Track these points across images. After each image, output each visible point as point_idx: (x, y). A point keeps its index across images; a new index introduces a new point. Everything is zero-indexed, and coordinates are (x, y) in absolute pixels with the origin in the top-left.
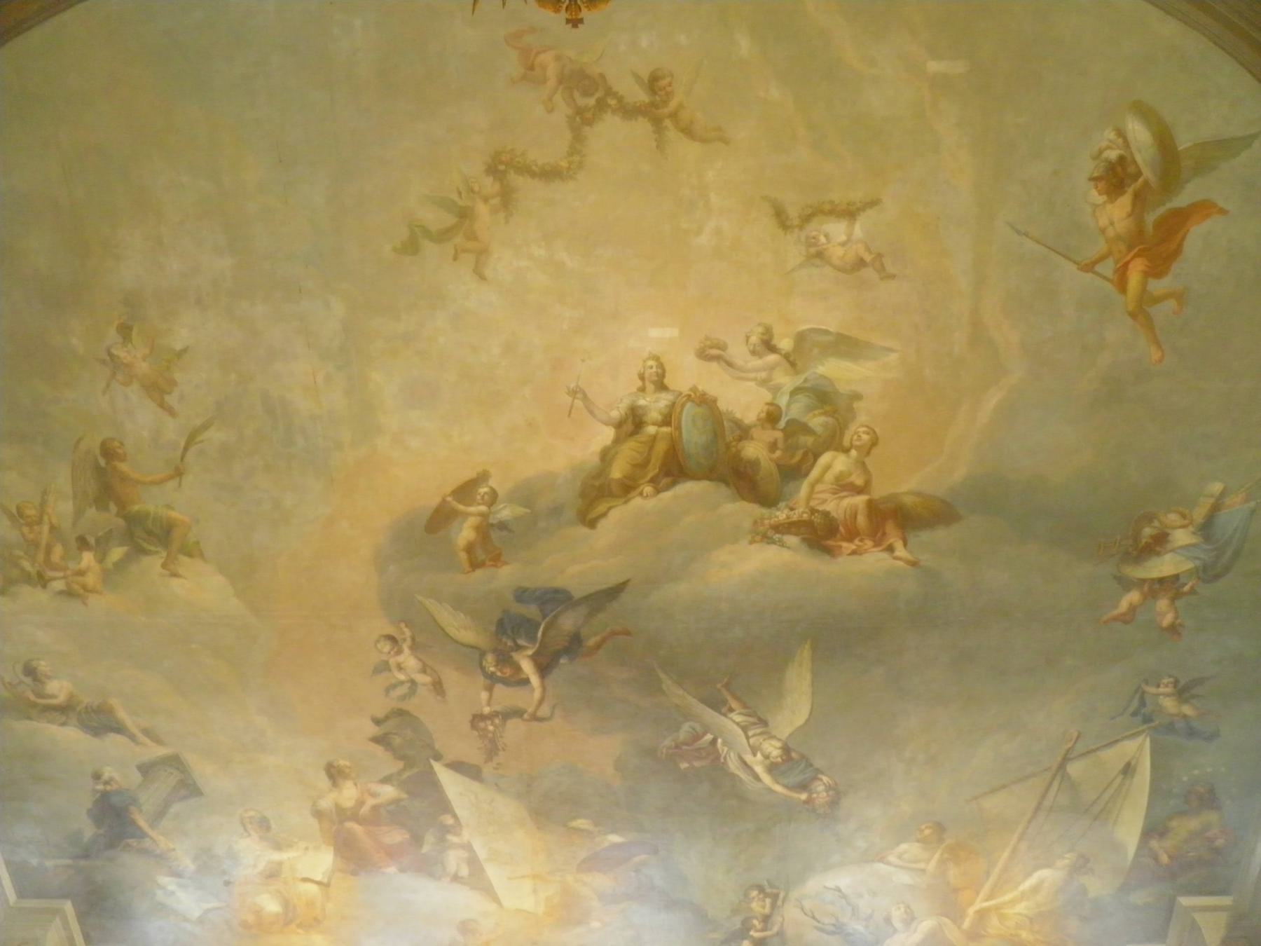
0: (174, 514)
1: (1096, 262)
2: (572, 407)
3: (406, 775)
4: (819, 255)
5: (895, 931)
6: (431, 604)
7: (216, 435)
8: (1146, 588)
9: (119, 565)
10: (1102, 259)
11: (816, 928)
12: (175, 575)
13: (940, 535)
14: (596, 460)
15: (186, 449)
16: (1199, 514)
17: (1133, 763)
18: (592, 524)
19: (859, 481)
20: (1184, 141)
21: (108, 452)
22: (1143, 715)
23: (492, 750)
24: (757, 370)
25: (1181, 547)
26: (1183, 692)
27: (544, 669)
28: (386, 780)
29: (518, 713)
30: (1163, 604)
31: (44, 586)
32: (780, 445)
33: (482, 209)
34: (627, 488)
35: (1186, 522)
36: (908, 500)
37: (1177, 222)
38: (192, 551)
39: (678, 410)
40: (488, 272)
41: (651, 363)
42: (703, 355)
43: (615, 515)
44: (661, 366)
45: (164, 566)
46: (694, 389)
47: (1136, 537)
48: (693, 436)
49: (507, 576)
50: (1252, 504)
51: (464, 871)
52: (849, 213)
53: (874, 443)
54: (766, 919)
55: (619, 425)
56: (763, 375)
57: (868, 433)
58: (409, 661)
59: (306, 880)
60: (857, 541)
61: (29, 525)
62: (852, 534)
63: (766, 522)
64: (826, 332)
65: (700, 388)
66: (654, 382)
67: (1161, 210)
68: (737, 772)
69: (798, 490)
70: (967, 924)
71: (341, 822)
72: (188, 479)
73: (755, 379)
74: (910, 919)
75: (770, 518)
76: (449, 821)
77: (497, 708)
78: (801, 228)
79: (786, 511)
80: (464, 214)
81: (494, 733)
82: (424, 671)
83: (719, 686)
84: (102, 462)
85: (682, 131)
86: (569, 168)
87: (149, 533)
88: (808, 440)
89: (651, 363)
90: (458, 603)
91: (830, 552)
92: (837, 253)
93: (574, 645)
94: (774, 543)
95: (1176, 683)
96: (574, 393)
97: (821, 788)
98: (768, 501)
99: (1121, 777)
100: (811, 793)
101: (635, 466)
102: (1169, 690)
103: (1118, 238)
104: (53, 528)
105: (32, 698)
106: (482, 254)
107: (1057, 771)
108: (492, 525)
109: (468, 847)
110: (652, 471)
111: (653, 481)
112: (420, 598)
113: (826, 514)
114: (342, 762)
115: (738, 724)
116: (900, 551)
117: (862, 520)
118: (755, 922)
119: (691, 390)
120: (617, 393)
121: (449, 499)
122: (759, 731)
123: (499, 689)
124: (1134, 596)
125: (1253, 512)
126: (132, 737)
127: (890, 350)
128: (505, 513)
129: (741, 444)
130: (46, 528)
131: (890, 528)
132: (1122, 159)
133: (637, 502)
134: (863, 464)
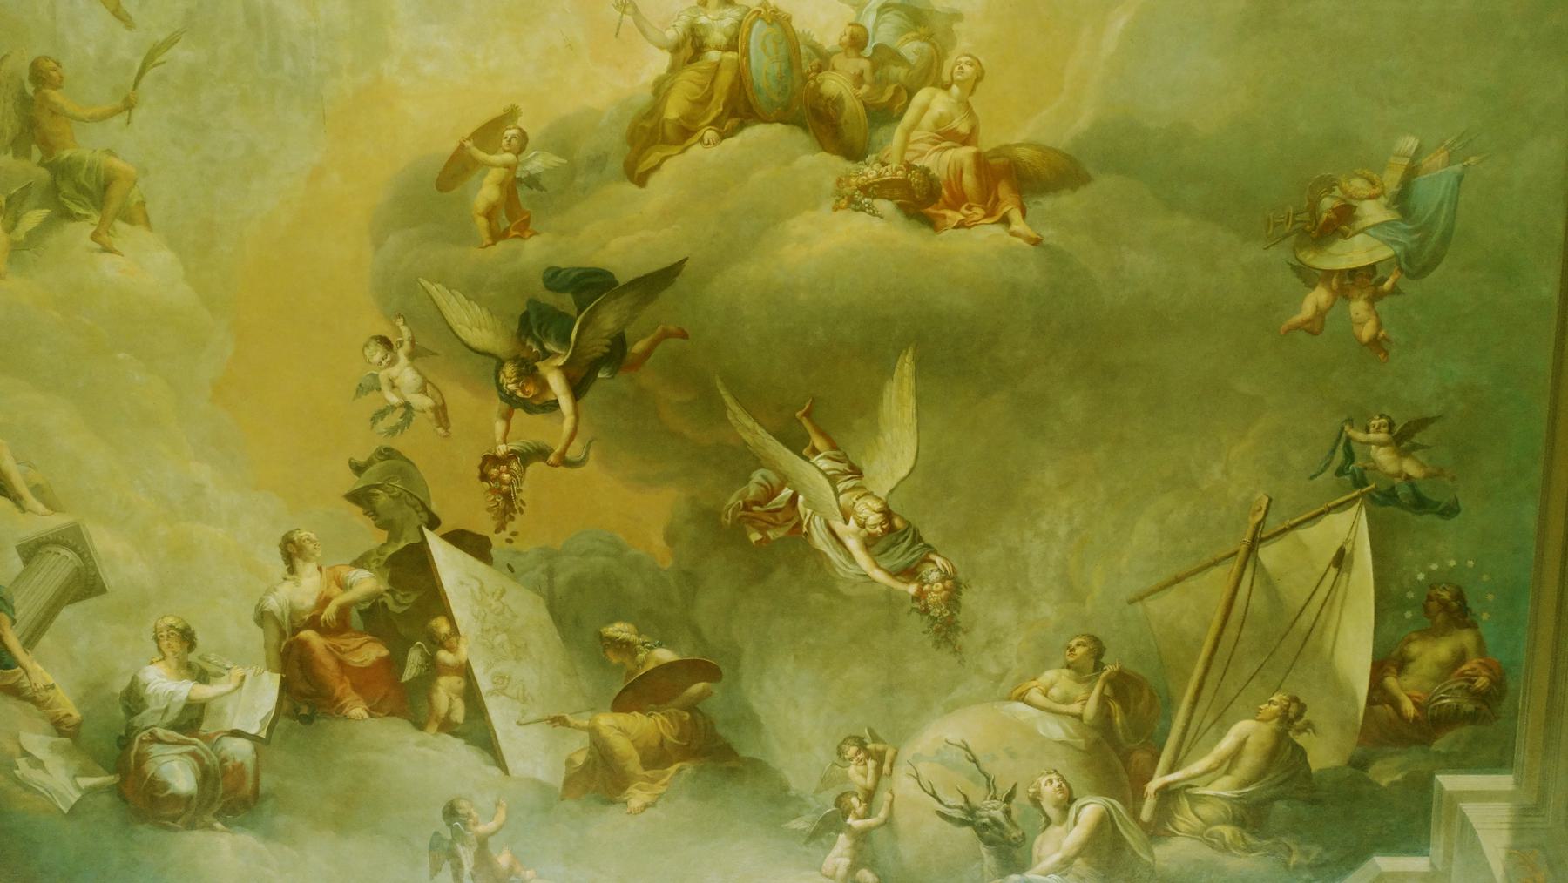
0: (117, 163)
3: (391, 551)
5: (1048, 822)
6: (436, 290)
7: (182, 54)
9: (34, 237)
12: (107, 249)
13: (1066, 202)
15: (141, 73)
16: (1392, 180)
17: (1348, 548)
18: (641, 181)
19: (964, 128)
21: (39, 75)
22: (1354, 478)
23: (507, 506)
25: (1374, 226)
26: (1402, 440)
28: (359, 563)
29: (541, 453)
30: (1358, 307)
32: (867, 76)
34: (686, 132)
35: (1377, 191)
36: (1024, 154)
39: (746, 30)
43: (670, 169)
45: (94, 237)
47: (1313, 209)
48: (764, 66)
49: (535, 251)
50: (1458, 168)
51: (459, 714)
53: (979, 78)
54: (869, 796)
55: (676, 49)
58: (405, 374)
59: (237, 734)
60: (963, 209)
63: (853, 181)
68: (824, 548)
69: (890, 139)
70: (1146, 814)
71: (296, 631)
72: (139, 113)
74: (1068, 802)
76: (442, 626)
79: (876, 166)
81: (511, 483)
83: (799, 414)
84: (30, 89)
87: (81, 189)
88: (899, 72)
90: (473, 290)
91: (931, 223)
93: (617, 353)
95: (1391, 425)
97: (934, 576)
98: (854, 153)
99: (1333, 571)
101: (694, 103)
102: (1382, 436)
108: (520, 180)
109: (465, 671)
110: (715, 110)
112: (425, 283)
113: (925, 171)
114: (304, 534)
115: (823, 472)
116: (1018, 225)
117: (969, 180)
118: (854, 800)
121: (468, 144)
122: (851, 483)
123: (519, 415)
124: (1319, 297)
125: (1460, 178)
126: (17, 500)
128: (537, 163)
131: (1003, 190)
133: (696, 150)
134: (968, 106)
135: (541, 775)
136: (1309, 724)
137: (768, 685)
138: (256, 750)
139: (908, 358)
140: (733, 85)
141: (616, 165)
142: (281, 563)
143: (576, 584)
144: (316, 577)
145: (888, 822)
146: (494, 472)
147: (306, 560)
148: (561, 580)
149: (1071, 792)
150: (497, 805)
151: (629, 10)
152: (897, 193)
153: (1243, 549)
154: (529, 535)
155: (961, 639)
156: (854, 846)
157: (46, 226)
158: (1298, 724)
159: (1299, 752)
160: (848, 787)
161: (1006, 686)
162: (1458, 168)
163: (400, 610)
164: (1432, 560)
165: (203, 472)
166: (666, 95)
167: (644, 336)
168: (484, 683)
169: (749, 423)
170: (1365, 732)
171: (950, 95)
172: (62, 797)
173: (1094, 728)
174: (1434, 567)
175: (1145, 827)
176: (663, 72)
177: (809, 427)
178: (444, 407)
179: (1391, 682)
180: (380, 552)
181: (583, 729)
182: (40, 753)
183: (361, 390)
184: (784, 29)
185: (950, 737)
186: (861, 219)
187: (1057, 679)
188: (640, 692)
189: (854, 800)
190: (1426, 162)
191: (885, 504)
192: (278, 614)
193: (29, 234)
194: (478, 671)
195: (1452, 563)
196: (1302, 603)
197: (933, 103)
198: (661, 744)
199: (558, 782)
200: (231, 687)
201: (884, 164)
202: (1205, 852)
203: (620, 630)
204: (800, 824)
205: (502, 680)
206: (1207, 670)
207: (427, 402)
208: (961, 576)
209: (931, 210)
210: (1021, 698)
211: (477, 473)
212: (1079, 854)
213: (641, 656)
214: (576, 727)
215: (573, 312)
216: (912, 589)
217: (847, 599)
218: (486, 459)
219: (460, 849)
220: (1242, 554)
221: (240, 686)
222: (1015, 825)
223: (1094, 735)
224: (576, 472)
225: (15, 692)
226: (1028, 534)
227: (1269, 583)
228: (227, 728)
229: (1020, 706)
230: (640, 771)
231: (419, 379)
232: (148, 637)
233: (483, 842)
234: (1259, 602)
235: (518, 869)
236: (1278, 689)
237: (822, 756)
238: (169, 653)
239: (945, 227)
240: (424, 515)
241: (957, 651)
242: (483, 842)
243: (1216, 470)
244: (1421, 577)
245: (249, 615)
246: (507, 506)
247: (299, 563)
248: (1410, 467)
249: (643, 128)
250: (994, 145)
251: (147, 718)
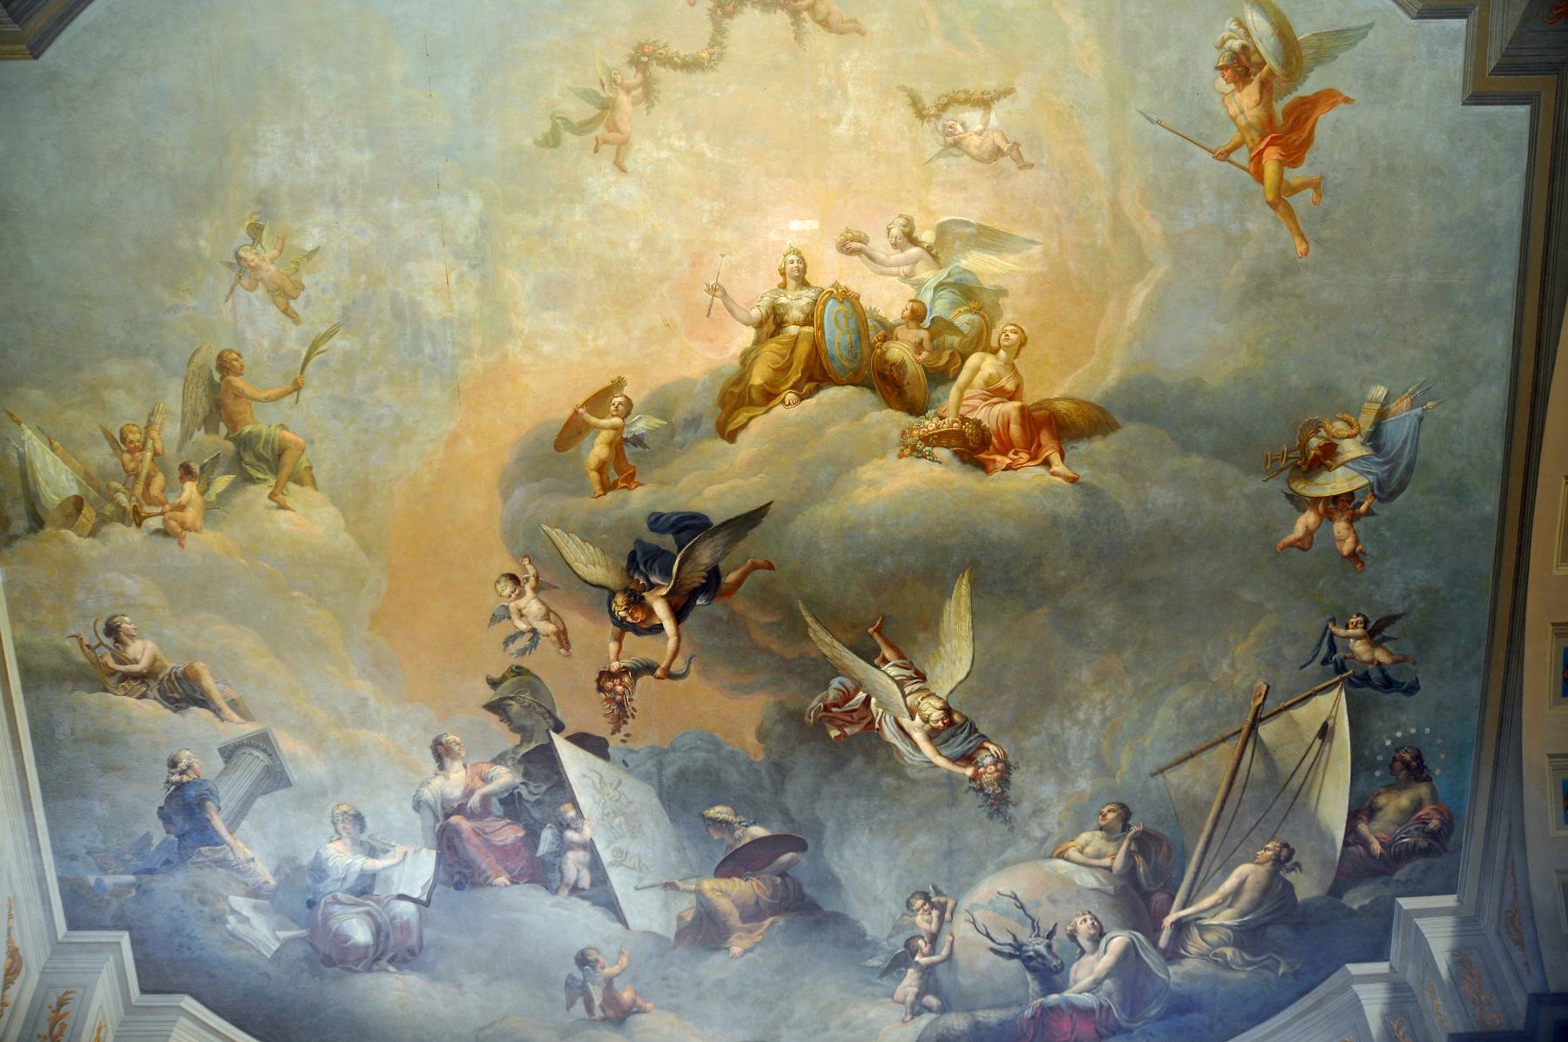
0: (287, 435)
1: (1229, 152)
3: (524, 750)
4: (957, 144)
5: (1083, 952)
6: (557, 535)
7: (340, 343)
8: (1321, 507)
9: (223, 497)
10: (1236, 147)
11: (992, 949)
12: (282, 507)
13: (1098, 446)
14: (736, 364)
15: (307, 360)
16: (1366, 422)
17: (1330, 723)
18: (731, 437)
19: (1010, 386)
20: (1303, 32)
21: (224, 365)
23: (621, 713)
25: (1352, 460)
26: (1374, 634)
27: (679, 614)
28: (495, 762)
31: (139, 525)
32: (926, 344)
33: (624, 100)
34: (769, 395)
36: (1062, 406)
37: (1303, 113)
38: (302, 478)
40: (628, 164)
41: (791, 257)
43: (755, 426)
44: (802, 260)
45: (271, 496)
46: (836, 285)
47: (1303, 447)
48: (837, 338)
49: (640, 500)
50: (1418, 411)
51: (585, 881)
52: (984, 102)
53: (1023, 343)
54: (934, 939)
55: (759, 325)
56: (906, 269)
58: (531, 604)
59: (402, 897)
60: (1011, 454)
61: (130, 451)
62: (1006, 447)
64: (968, 224)
66: (795, 279)
67: (1288, 99)
68: (893, 741)
70: (1163, 942)
71: (447, 816)
72: (306, 394)
74: (1099, 935)
77: (626, 662)
78: (938, 117)
80: (607, 106)
82: (547, 617)
84: (217, 377)
85: (819, 22)
86: (710, 60)
87: (259, 457)
88: (953, 340)
89: (791, 257)
90: (588, 533)
91: (983, 466)
92: (973, 142)
95: (1366, 622)
96: (712, 290)
97: (988, 760)
98: (916, 409)
99: (1318, 742)
100: (977, 766)
102: (1359, 631)
103: (1250, 126)
104: (156, 454)
105: (111, 663)
106: (623, 145)
107: (1249, 735)
108: (626, 440)
109: (589, 847)
110: (795, 376)
112: (546, 528)
113: (978, 423)
114: (451, 738)
115: (892, 678)
116: (1058, 466)
117: (1015, 429)
118: (921, 942)
120: (757, 289)
121: (581, 410)
122: (917, 686)
123: (629, 637)
124: (1309, 519)
125: (1421, 419)
126: (217, 712)
128: (640, 425)
130: (149, 455)
131: (1045, 437)
132: (1244, 48)
133: (779, 410)
135: (656, 928)
136: (1297, 864)
137: (847, 853)
138: (420, 911)
139: (965, 581)
140: (809, 356)
141: (709, 425)
142: (433, 760)
143: (682, 775)
144: (462, 773)
145: (950, 957)
146: (609, 685)
147: (454, 759)
148: (670, 771)
149: (1101, 928)
150: (621, 953)
152: (954, 442)
153: (1246, 727)
154: (644, 734)
155: (1011, 810)
156: (921, 978)
157: (233, 488)
158: (1288, 865)
159: (1289, 887)
160: (916, 932)
161: (1049, 846)
162: (1418, 411)
163: (532, 799)
164: (1397, 728)
165: (365, 688)
166: (751, 366)
167: (735, 569)
168: (606, 857)
169: (828, 639)
170: (1340, 871)
172: (268, 949)
173: (1121, 876)
174: (1399, 734)
175: (1163, 952)
176: (749, 345)
177: (879, 641)
178: (565, 632)
179: (1363, 828)
180: (514, 751)
181: (690, 892)
182: (246, 911)
183: (495, 619)
184: (853, 305)
185: (1001, 890)
187: (1092, 840)
188: (738, 862)
189: (921, 942)
190: (1392, 406)
191: (946, 703)
192: (432, 802)
193: (219, 496)
194: (600, 847)
195: (1413, 731)
196: (1292, 769)
197: (982, 366)
198: (757, 902)
199: (672, 936)
200: (395, 861)
201: (942, 418)
202: (1209, 969)
203: (720, 812)
204: (874, 962)
205: (621, 856)
206: (1215, 825)
207: (550, 628)
208: (1011, 759)
209: (983, 456)
210: (1061, 856)
211: (595, 685)
212: (1107, 976)
213: (738, 833)
214: (685, 891)
215: (674, 549)
216: (969, 771)
217: (914, 782)
218: (602, 674)
219: (591, 987)
220: (1244, 732)
221: (403, 860)
222: (1055, 956)
223: (1120, 883)
224: (680, 683)
225: (222, 863)
226: (1067, 723)
227: (1267, 754)
228: (395, 893)
229: (1061, 862)
230: (739, 924)
231: (543, 609)
232: (327, 820)
233: (609, 982)
234: (1258, 770)
235: (640, 1002)
236: (1271, 839)
237: (894, 907)
238: (344, 833)
239: (995, 469)
240: (551, 722)
241: (1008, 820)
242: (609, 982)
243: (1225, 665)
244: (1388, 743)
245: (408, 806)
246: (621, 713)
247: (448, 761)
248: (1381, 655)
251: (328, 886)
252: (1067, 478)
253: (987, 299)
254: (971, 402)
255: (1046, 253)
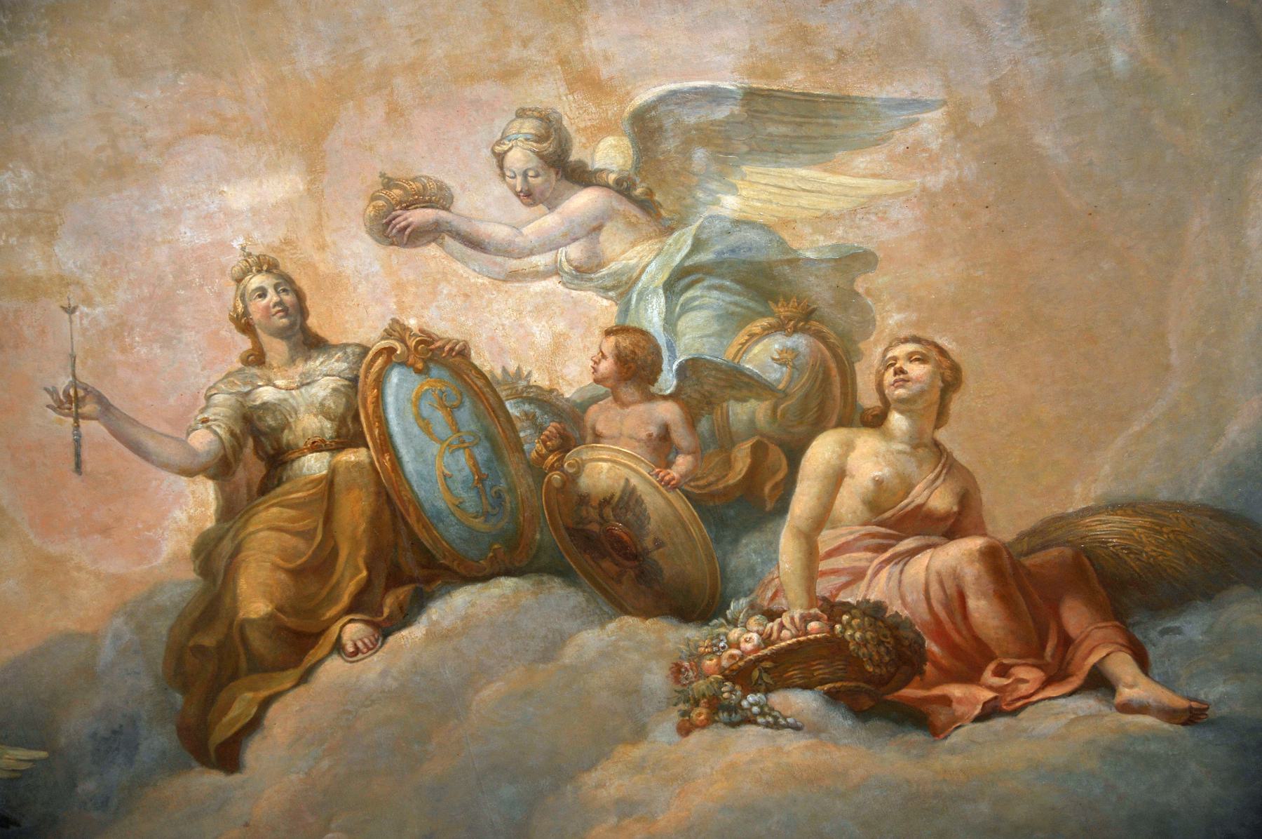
2: (78, 443)
14: (189, 574)
18: (228, 758)
19: (942, 501)
24: (550, 245)
32: (680, 435)
34: (297, 641)
36: (1108, 528)
41: (256, 281)
42: (392, 230)
44: (287, 283)
46: (397, 330)
53: (951, 379)
55: (221, 468)
56: (575, 252)
57: (923, 360)
60: (988, 676)
62: (970, 660)
63: (709, 663)
64: (714, 96)
65: (412, 323)
66: (281, 333)
69: (771, 558)
73: (555, 271)
75: (715, 652)
88: (745, 412)
89: (256, 281)
91: (921, 720)
94: (750, 720)
96: (73, 402)
98: (698, 604)
101: (297, 574)
111: (360, 605)
113: (875, 612)
116: (1134, 685)
119: (388, 334)
120: (192, 378)
127: (925, 106)
129: (571, 457)
131: (1075, 616)
133: (334, 669)
140: (375, 521)
141: (159, 740)
151: (89, 408)
152: (820, 670)
171: (888, 436)
176: (210, 524)
184: (457, 373)
186: (749, 743)
201: (771, 615)
209: (911, 692)
239: (955, 722)
249: (200, 650)
250: (1027, 524)
252: (1169, 714)
253: (819, 291)
254: (841, 562)
255: (959, 126)
